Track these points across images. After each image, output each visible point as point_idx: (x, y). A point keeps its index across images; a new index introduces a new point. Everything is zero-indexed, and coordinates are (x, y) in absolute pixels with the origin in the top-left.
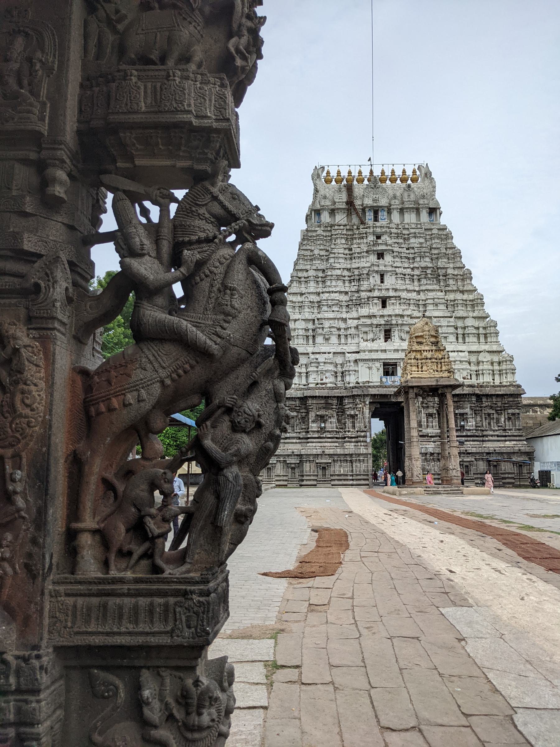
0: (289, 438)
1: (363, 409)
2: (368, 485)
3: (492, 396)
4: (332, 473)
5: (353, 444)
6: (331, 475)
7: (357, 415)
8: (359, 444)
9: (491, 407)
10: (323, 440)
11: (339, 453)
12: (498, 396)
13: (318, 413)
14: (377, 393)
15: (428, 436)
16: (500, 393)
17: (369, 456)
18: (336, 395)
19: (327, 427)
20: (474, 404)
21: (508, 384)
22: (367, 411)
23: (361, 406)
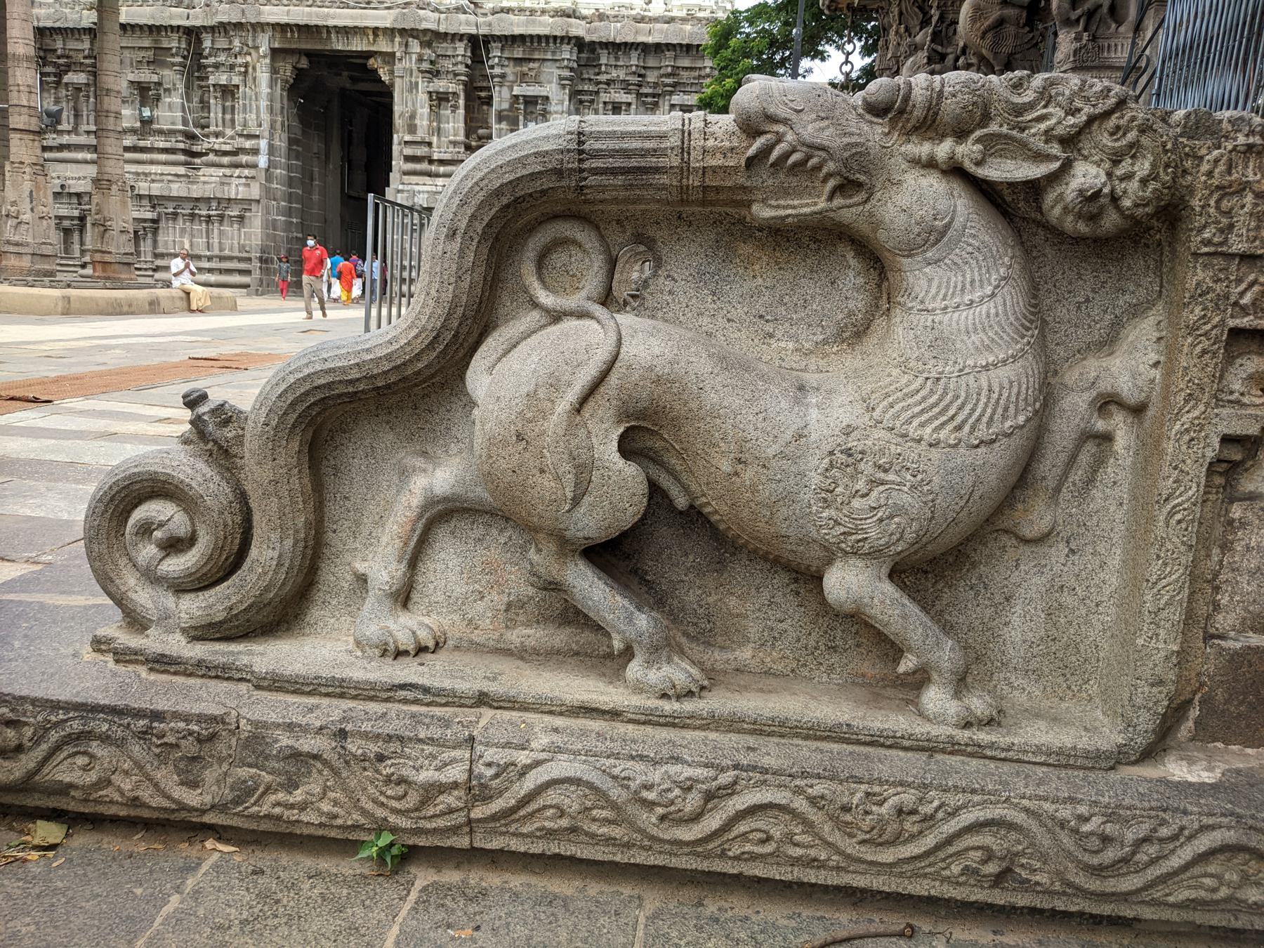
0: (67, 147)
1: (254, 68)
2: (246, 286)
3: (626, 47)
4: (160, 250)
5: (221, 172)
6: (156, 256)
7: (238, 86)
8: (237, 172)
9: (626, 86)
10: (144, 156)
11: (174, 194)
12: (645, 49)
13: (131, 77)
14: (284, 20)
15: (431, 162)
16: (650, 40)
17: (254, 207)
18: (175, 23)
19: (161, 121)
20: (572, 69)
21: (683, 14)
22: (263, 77)
23: (248, 58)
